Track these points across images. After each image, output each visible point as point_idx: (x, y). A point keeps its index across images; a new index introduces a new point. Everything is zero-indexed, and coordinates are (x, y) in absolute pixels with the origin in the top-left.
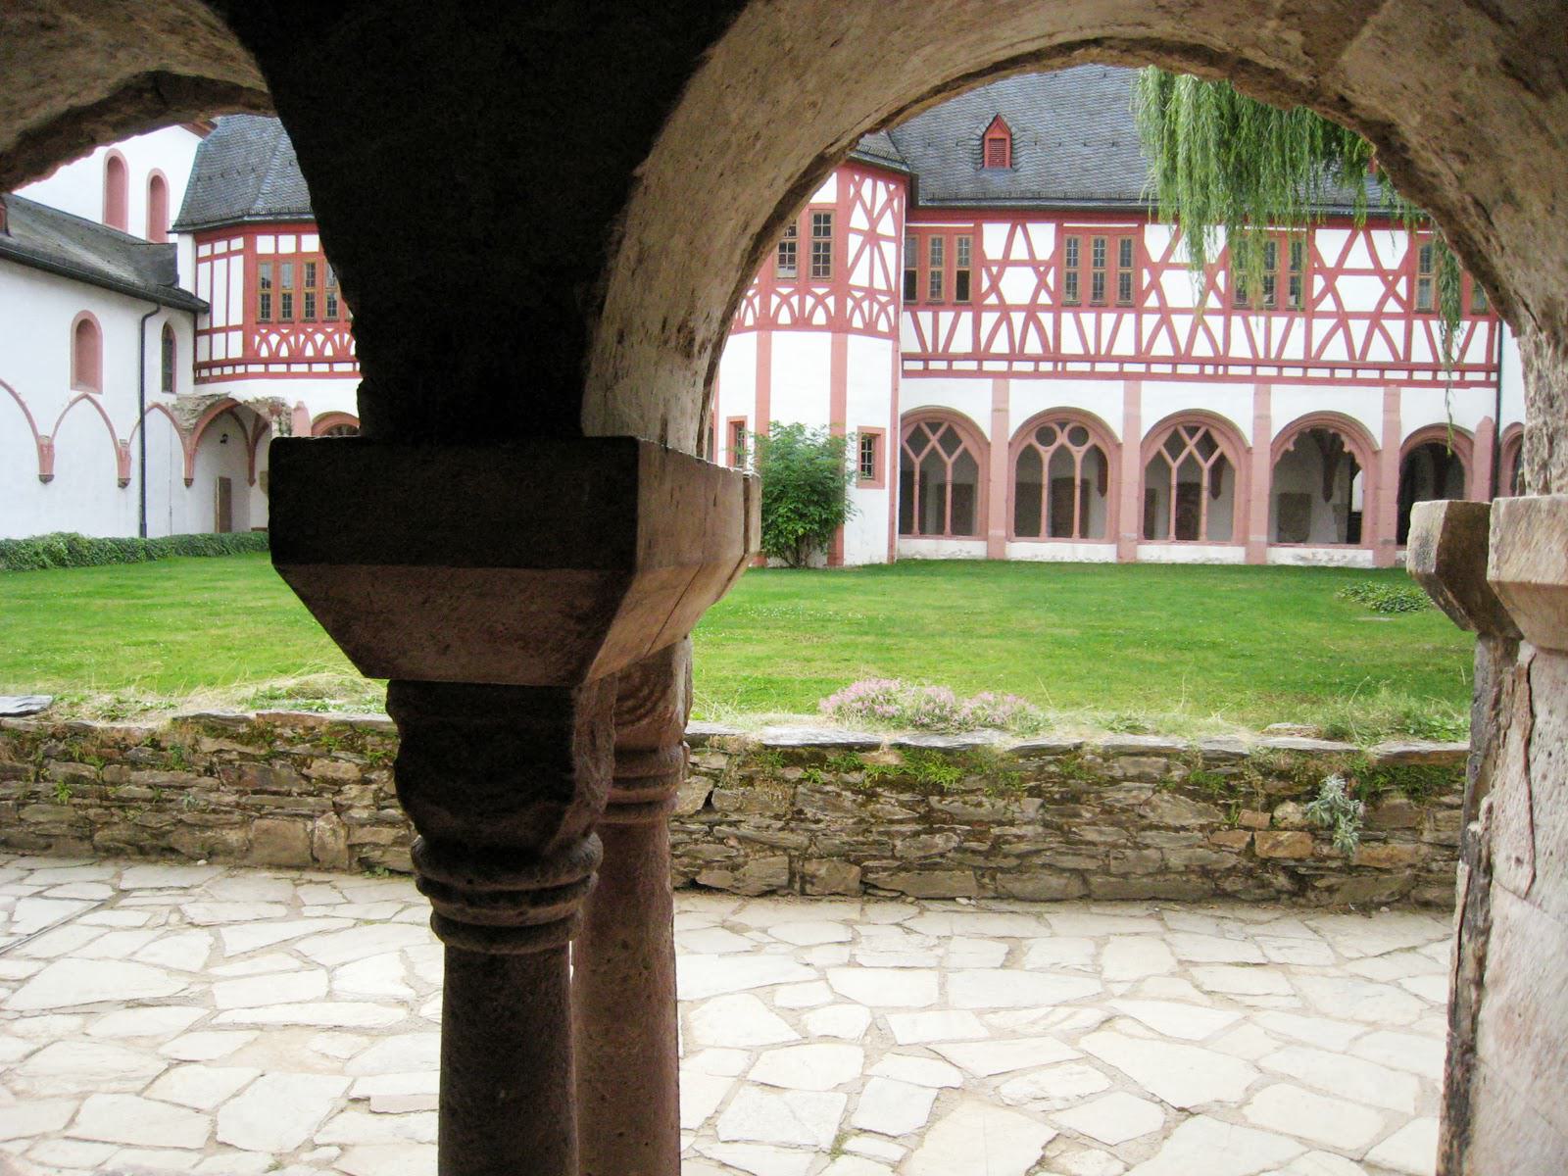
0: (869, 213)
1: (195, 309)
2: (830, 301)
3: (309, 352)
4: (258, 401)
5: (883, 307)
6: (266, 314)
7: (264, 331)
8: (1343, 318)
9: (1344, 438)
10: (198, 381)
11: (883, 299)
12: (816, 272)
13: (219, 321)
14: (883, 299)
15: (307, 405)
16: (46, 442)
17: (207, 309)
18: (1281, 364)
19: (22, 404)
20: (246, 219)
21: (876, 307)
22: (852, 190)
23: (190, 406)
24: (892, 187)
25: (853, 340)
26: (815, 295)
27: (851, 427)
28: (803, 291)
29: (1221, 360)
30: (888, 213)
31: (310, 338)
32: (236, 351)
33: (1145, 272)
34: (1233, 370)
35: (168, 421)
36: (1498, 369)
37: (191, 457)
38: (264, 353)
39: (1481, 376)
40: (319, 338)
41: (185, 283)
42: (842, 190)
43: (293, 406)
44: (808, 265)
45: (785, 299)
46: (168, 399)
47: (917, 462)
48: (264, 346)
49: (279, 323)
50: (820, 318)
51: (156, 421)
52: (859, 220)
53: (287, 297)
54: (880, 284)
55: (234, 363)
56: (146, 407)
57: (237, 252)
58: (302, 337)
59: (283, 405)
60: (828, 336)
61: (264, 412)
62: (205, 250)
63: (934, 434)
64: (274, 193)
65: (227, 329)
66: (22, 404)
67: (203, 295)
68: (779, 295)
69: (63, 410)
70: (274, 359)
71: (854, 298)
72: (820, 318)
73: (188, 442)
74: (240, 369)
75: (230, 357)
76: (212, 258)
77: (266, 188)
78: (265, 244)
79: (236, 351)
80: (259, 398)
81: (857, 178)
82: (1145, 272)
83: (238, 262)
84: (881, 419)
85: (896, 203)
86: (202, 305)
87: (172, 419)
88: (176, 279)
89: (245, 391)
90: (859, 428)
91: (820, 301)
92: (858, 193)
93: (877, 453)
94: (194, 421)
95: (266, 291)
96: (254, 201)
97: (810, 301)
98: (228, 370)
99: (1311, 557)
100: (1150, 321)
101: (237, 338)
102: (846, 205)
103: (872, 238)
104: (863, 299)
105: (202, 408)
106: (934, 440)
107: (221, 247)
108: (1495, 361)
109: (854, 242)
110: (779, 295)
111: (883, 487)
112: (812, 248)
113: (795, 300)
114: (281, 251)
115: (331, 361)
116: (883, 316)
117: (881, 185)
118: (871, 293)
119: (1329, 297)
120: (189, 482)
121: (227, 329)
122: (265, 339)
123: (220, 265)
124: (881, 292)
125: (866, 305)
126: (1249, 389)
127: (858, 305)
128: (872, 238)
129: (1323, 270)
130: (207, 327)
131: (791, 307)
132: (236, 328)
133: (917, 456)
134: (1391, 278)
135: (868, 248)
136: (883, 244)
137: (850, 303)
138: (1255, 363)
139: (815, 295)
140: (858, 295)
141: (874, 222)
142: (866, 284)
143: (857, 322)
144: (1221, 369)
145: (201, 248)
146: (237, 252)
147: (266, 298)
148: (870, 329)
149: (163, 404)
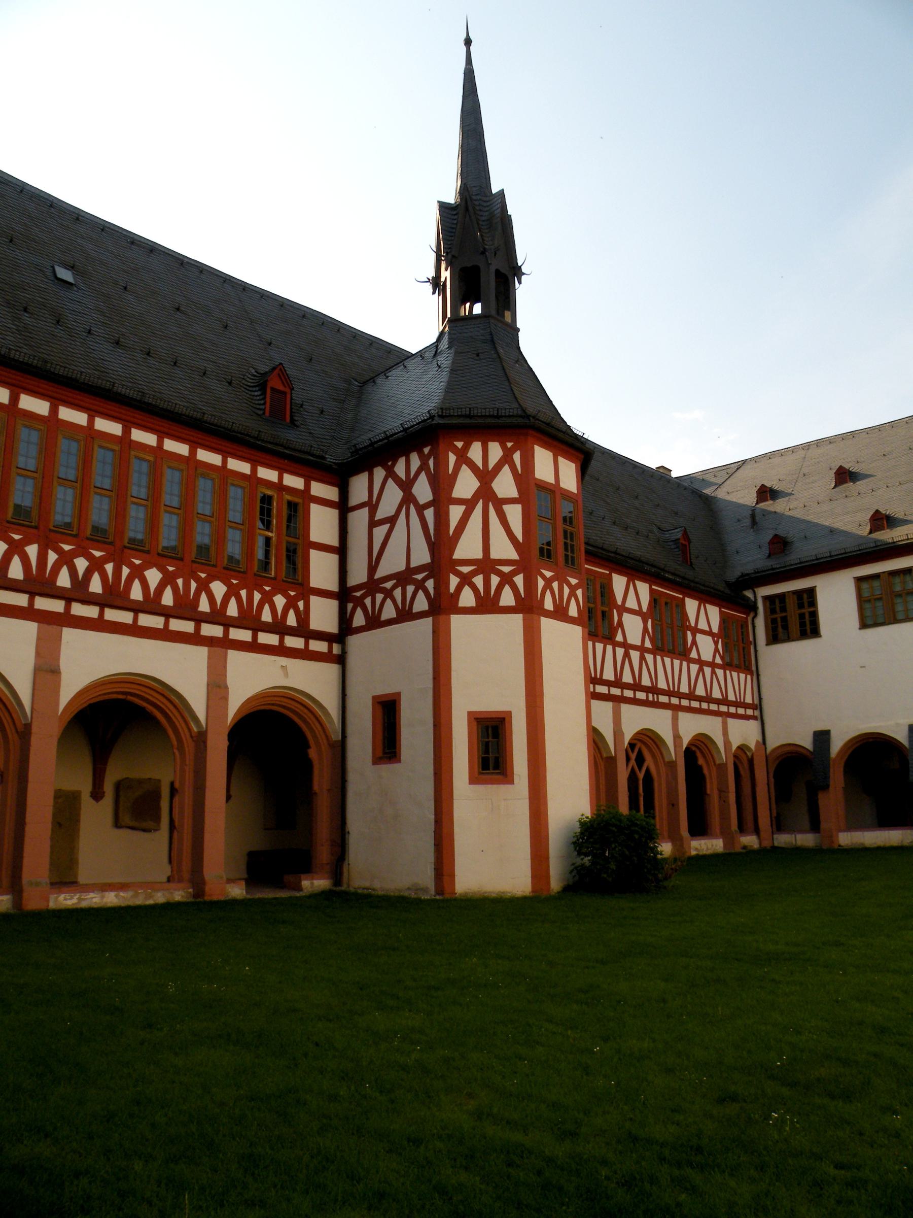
8: (701, 663)
9: (698, 754)
18: (681, 696)
29: (654, 689)
33: (615, 611)
34: (663, 699)
36: (758, 706)
39: (750, 712)
82: (615, 611)
99: (699, 847)
100: (620, 652)
108: (756, 702)
119: (694, 648)
126: (668, 713)
129: (689, 628)
134: (716, 639)
138: (669, 693)
144: (651, 698)
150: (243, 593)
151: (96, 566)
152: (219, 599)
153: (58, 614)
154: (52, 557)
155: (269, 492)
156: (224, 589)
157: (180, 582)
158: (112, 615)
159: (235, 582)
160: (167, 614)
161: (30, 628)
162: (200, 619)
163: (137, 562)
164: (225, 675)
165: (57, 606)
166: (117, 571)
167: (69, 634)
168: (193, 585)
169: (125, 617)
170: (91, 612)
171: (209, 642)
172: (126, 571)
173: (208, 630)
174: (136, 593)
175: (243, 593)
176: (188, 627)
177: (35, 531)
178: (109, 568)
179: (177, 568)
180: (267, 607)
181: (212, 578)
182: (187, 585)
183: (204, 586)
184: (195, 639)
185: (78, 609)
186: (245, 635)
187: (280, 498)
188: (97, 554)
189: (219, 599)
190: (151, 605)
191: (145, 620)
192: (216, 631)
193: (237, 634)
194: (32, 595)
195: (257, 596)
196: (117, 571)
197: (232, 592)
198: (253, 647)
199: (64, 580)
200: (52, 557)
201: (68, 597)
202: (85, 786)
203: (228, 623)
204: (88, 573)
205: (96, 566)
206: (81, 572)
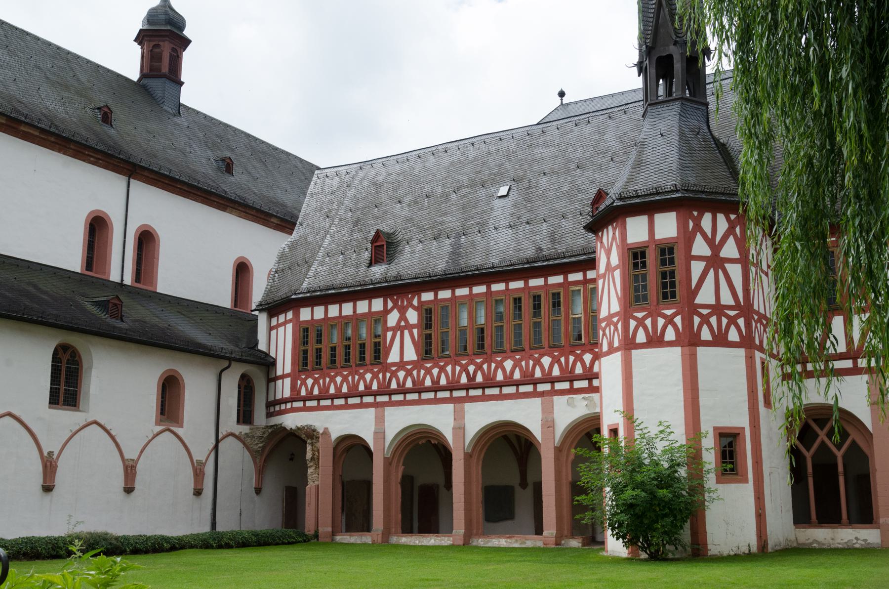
0: (710, 242)
1: (267, 363)
2: (678, 320)
3: (332, 390)
4: (298, 428)
5: (732, 321)
6: (305, 364)
7: (303, 377)
10: (269, 415)
11: (732, 313)
12: (665, 296)
13: (279, 372)
14: (732, 313)
15: (330, 430)
16: (131, 463)
17: (273, 363)
19: (113, 438)
20: (293, 297)
21: (725, 321)
22: (691, 224)
23: (259, 434)
24: (733, 217)
25: (701, 351)
26: (664, 316)
27: (707, 426)
28: (654, 314)
30: (731, 240)
31: (333, 379)
32: (287, 394)
35: (241, 445)
37: (260, 472)
38: (303, 393)
40: (339, 379)
41: (262, 346)
42: (682, 225)
43: (321, 432)
44: (657, 290)
45: (641, 323)
46: (244, 429)
47: (808, 455)
48: (303, 388)
49: (313, 370)
50: (670, 335)
51: (232, 451)
52: (700, 247)
53: (333, 349)
54: (727, 299)
55: (285, 401)
56: (220, 436)
57: (290, 321)
58: (328, 380)
59: (314, 430)
60: (678, 350)
61: (303, 436)
62: (274, 322)
63: (822, 429)
64: (315, 275)
65: (283, 377)
66: (113, 438)
67: (273, 354)
68: (636, 319)
69: (147, 440)
70: (310, 397)
71: (700, 315)
72: (670, 335)
73: (258, 461)
74: (289, 406)
75: (284, 397)
76: (278, 326)
77: (311, 273)
78: (305, 314)
79: (287, 394)
80: (299, 426)
81: (695, 213)
83: (290, 327)
84: (740, 419)
85: (738, 230)
86: (272, 360)
87: (244, 444)
88: (256, 343)
89: (291, 421)
90: (715, 429)
91: (670, 321)
92: (698, 228)
93: (738, 450)
94: (261, 445)
95: (319, 346)
96: (302, 284)
97: (661, 322)
98: (283, 407)
101: (288, 381)
102: (687, 238)
103: (715, 262)
104: (710, 315)
105: (265, 435)
106: (822, 435)
107: (282, 318)
109: (697, 268)
110: (636, 319)
111: (746, 481)
112: (660, 277)
113: (648, 322)
114: (315, 318)
115: (346, 397)
116: (733, 328)
117: (721, 218)
118: (718, 309)
120: (258, 491)
121: (283, 377)
122: (304, 383)
123: (281, 329)
124: (730, 308)
125: (713, 320)
127: (705, 320)
128: (715, 262)
130: (274, 376)
131: (646, 328)
132: (287, 376)
133: (808, 450)
135: (712, 271)
136: (727, 265)
137: (697, 320)
139: (664, 316)
140: (705, 312)
141: (716, 248)
142: (712, 301)
143: (706, 335)
145: (272, 319)
146: (290, 321)
147: (305, 352)
148: (720, 340)
149: (237, 433)
150: (563, 360)
151: (479, 367)
152: (546, 366)
153: (463, 397)
154: (458, 368)
155: (577, 288)
156: (551, 359)
157: (523, 363)
158: (488, 392)
159: (556, 354)
160: (517, 384)
161: (450, 407)
162: (535, 383)
163: (499, 359)
164: (552, 412)
165: (462, 393)
166: (489, 367)
167: (468, 406)
168: (531, 363)
169: (496, 391)
170: (478, 392)
171: (543, 394)
172: (493, 365)
173: (541, 388)
174: (500, 377)
175: (563, 360)
176: (529, 388)
177: (449, 359)
178: (485, 366)
179: (522, 356)
180: (579, 364)
181: (542, 355)
182: (527, 364)
183: (538, 362)
184: (534, 394)
185: (473, 393)
186: (566, 385)
187: (585, 289)
188: (478, 361)
189: (546, 366)
190: (509, 382)
191: (506, 390)
192: (546, 387)
193: (559, 386)
194: (451, 391)
195: (572, 358)
196: (489, 367)
197: (555, 360)
198: (572, 391)
199: (464, 380)
200: (458, 368)
201: (467, 388)
202: (513, 479)
203: (553, 381)
204: (475, 372)
205: (479, 367)
206: (471, 372)
